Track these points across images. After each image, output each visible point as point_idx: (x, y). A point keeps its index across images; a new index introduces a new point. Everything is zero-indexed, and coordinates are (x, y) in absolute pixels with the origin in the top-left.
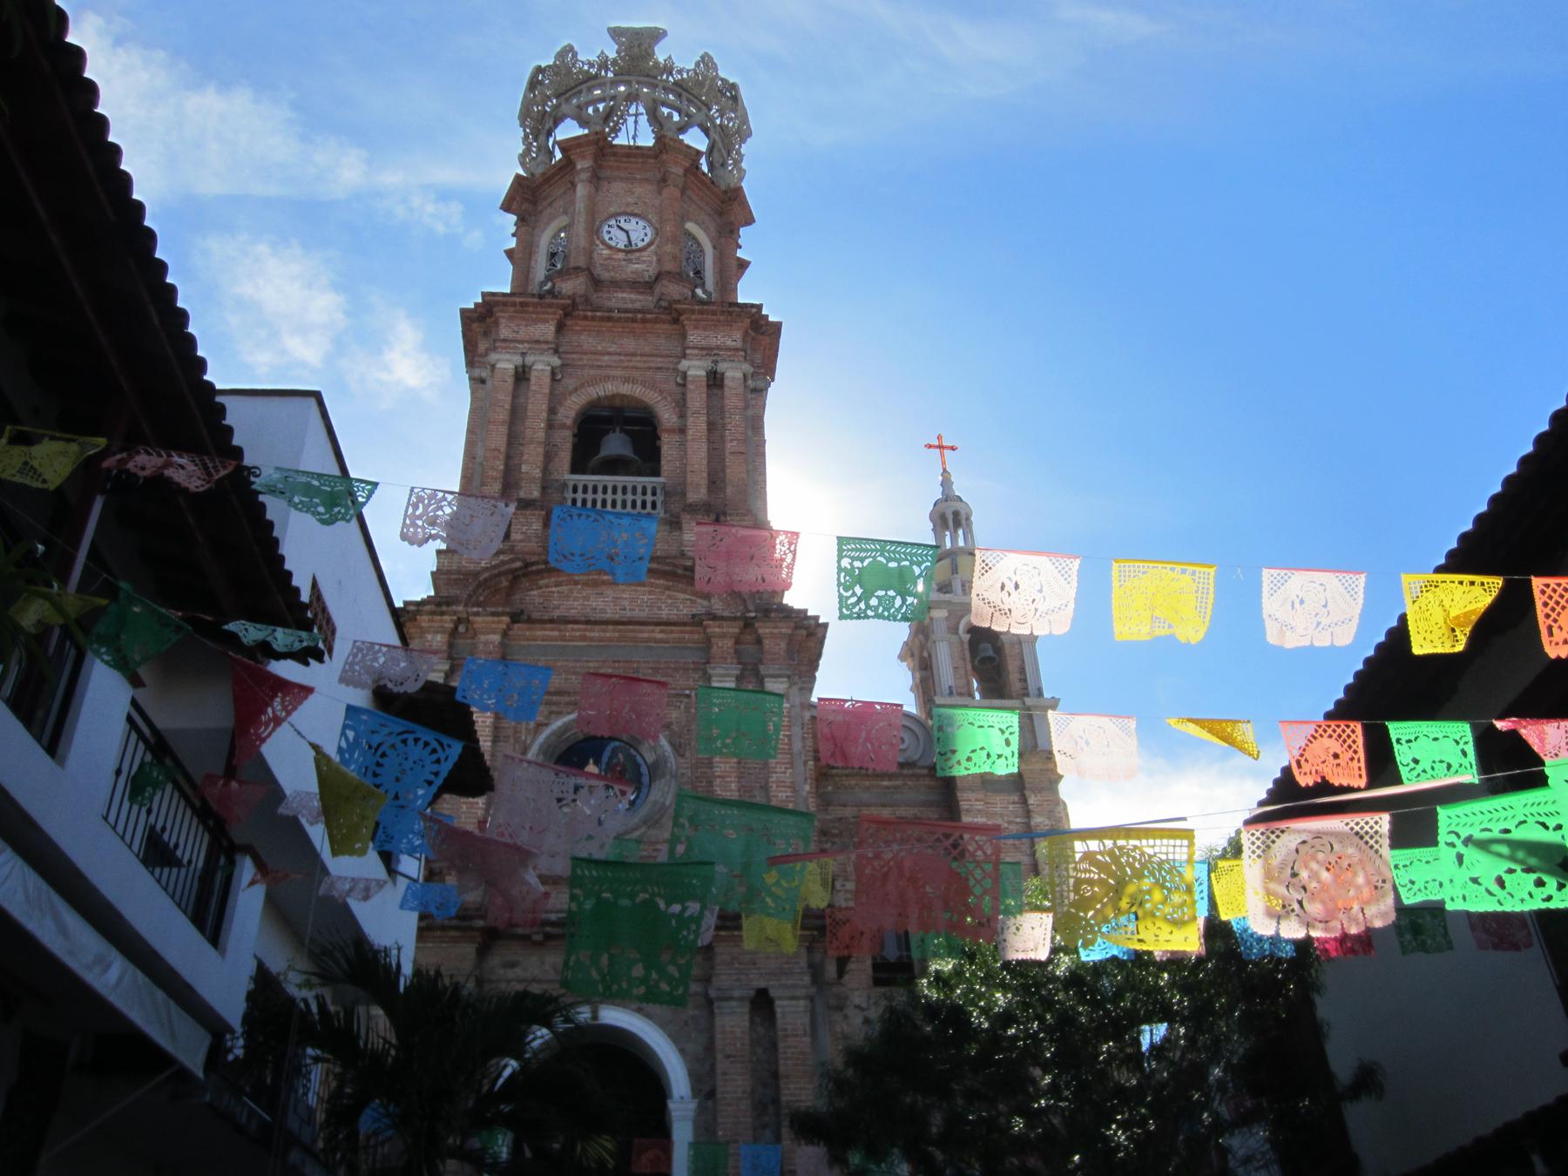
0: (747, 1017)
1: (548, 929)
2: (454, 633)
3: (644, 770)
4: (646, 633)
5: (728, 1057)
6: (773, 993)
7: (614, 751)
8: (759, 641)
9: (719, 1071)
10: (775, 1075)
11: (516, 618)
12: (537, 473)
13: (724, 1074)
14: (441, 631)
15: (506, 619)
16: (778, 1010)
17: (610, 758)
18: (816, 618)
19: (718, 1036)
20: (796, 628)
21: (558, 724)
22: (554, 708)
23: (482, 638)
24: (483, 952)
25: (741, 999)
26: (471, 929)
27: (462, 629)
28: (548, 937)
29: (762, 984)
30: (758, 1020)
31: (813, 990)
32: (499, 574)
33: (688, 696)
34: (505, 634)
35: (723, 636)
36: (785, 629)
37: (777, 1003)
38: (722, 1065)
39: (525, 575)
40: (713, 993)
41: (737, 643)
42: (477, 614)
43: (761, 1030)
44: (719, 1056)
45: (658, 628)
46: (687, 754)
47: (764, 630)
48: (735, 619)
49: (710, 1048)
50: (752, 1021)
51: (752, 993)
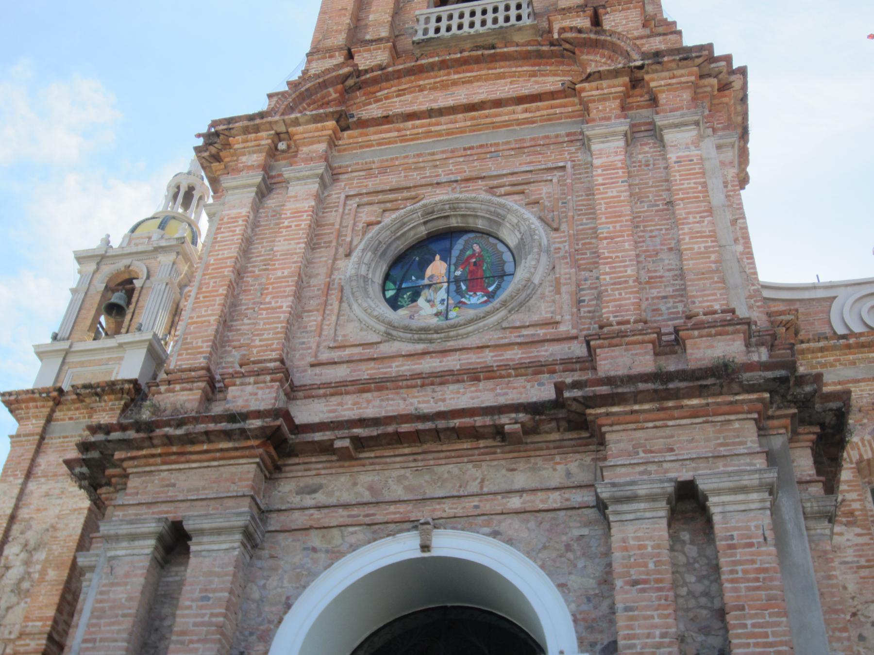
0: (664, 523)
1: (357, 431)
2: (273, 152)
3: (507, 256)
4: (505, 114)
5: (635, 583)
6: (703, 485)
7: (466, 242)
8: (654, 101)
9: (619, 606)
10: (721, 614)
11: (344, 122)
12: (387, 18)
13: (627, 609)
14: (257, 149)
15: (331, 123)
16: (714, 510)
17: (463, 251)
18: (728, 59)
19: (617, 555)
20: (702, 77)
21: (388, 219)
22: (389, 205)
23: (305, 149)
24: (272, 471)
25: (652, 498)
26: (244, 433)
27: (282, 146)
28: (360, 443)
29: (685, 475)
30: (686, 536)
31: (771, 476)
32: (324, 85)
33: (563, 168)
34: (332, 143)
35: (604, 98)
36: (687, 75)
37: (712, 500)
38: (623, 595)
39: (358, 87)
40: (605, 493)
41: (623, 108)
42: (296, 122)
43: (692, 551)
44: (619, 583)
45: (520, 108)
46: (564, 227)
47: (656, 81)
48: (615, 73)
49: (606, 581)
50: (674, 538)
51: (670, 488)
